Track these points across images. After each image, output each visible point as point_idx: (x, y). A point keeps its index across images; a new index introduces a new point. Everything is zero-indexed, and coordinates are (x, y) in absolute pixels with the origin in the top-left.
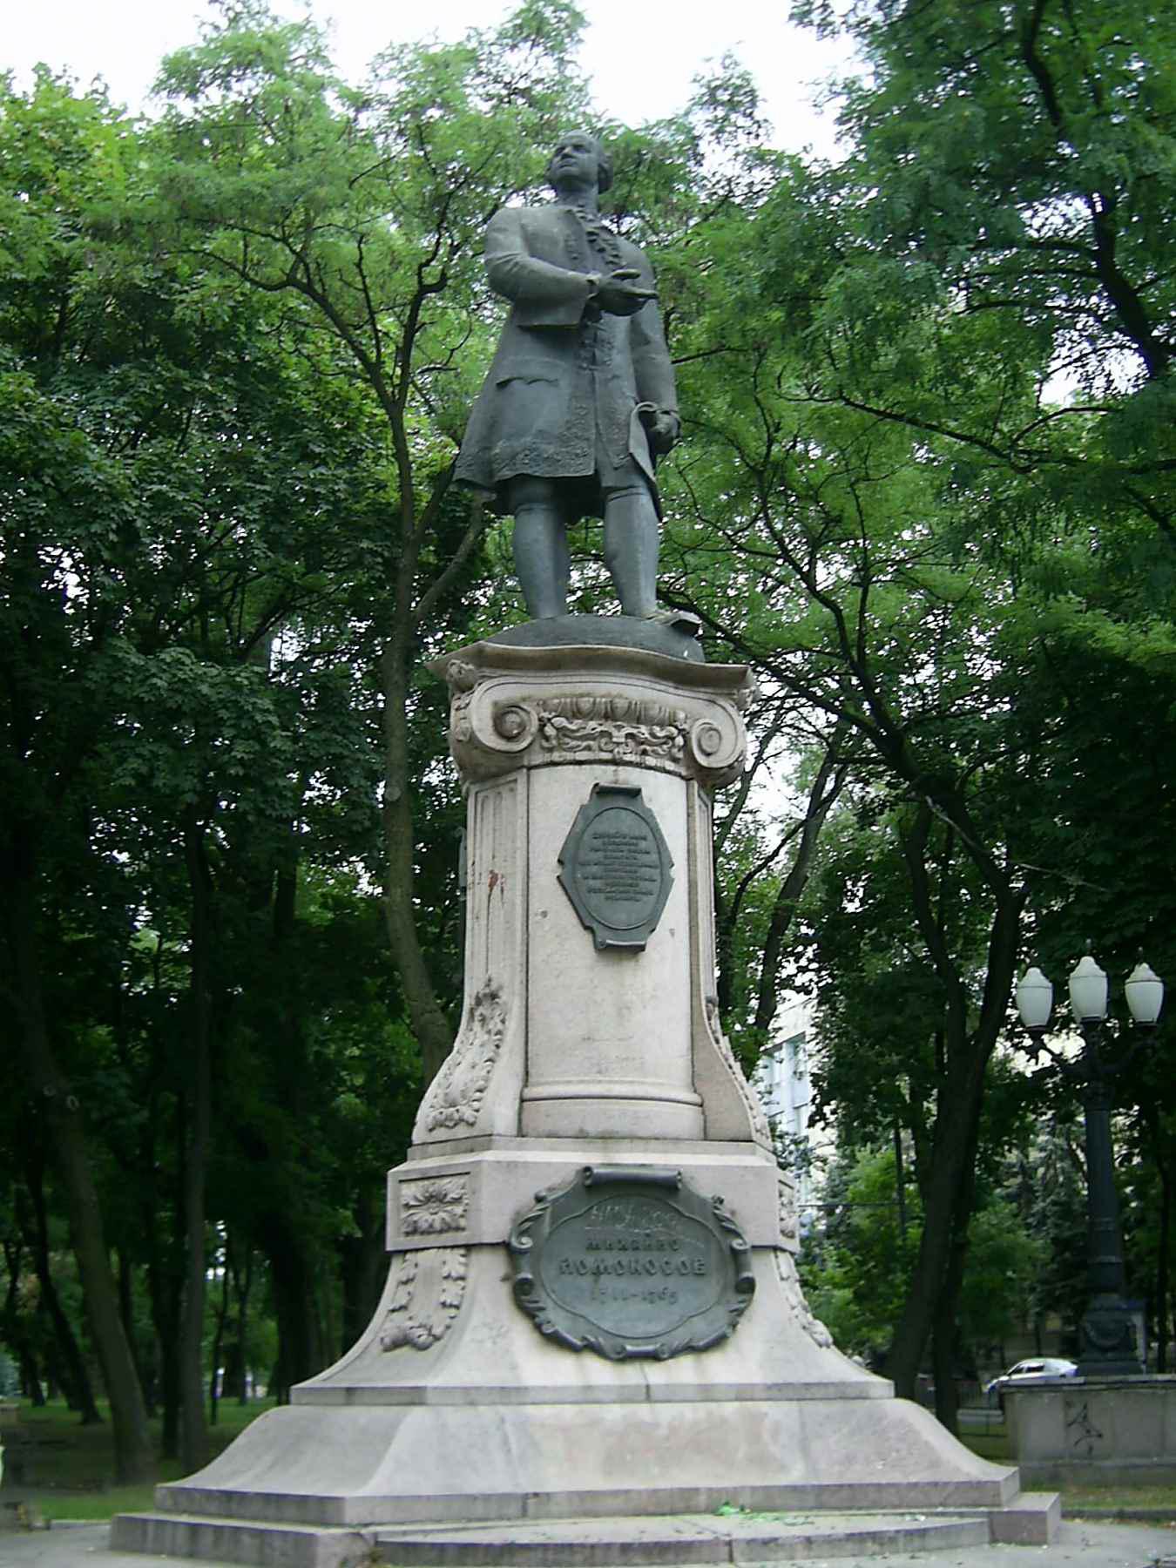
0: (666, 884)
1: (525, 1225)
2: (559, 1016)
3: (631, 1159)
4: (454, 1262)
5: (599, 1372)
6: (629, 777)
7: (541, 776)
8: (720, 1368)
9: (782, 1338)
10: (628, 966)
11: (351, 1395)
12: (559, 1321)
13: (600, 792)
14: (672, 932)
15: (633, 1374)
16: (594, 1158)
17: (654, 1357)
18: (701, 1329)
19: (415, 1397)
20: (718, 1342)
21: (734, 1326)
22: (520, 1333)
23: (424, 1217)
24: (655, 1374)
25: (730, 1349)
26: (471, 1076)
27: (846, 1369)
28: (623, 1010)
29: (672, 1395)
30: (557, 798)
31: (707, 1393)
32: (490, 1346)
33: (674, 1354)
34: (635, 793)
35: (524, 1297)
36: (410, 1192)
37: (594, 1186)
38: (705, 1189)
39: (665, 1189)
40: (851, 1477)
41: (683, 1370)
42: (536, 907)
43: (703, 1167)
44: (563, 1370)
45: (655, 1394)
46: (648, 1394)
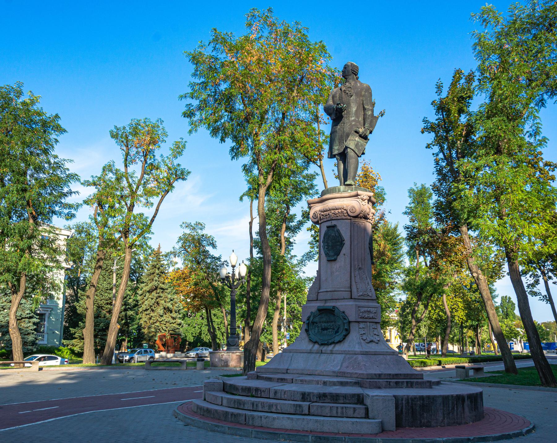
5: (317, 346)
8: (338, 347)
10: (333, 263)
13: (328, 227)
14: (344, 255)
18: (337, 339)
20: (340, 342)
21: (344, 339)
24: (324, 348)
25: (342, 344)
33: (331, 344)
34: (334, 226)
41: (330, 347)
45: (323, 352)
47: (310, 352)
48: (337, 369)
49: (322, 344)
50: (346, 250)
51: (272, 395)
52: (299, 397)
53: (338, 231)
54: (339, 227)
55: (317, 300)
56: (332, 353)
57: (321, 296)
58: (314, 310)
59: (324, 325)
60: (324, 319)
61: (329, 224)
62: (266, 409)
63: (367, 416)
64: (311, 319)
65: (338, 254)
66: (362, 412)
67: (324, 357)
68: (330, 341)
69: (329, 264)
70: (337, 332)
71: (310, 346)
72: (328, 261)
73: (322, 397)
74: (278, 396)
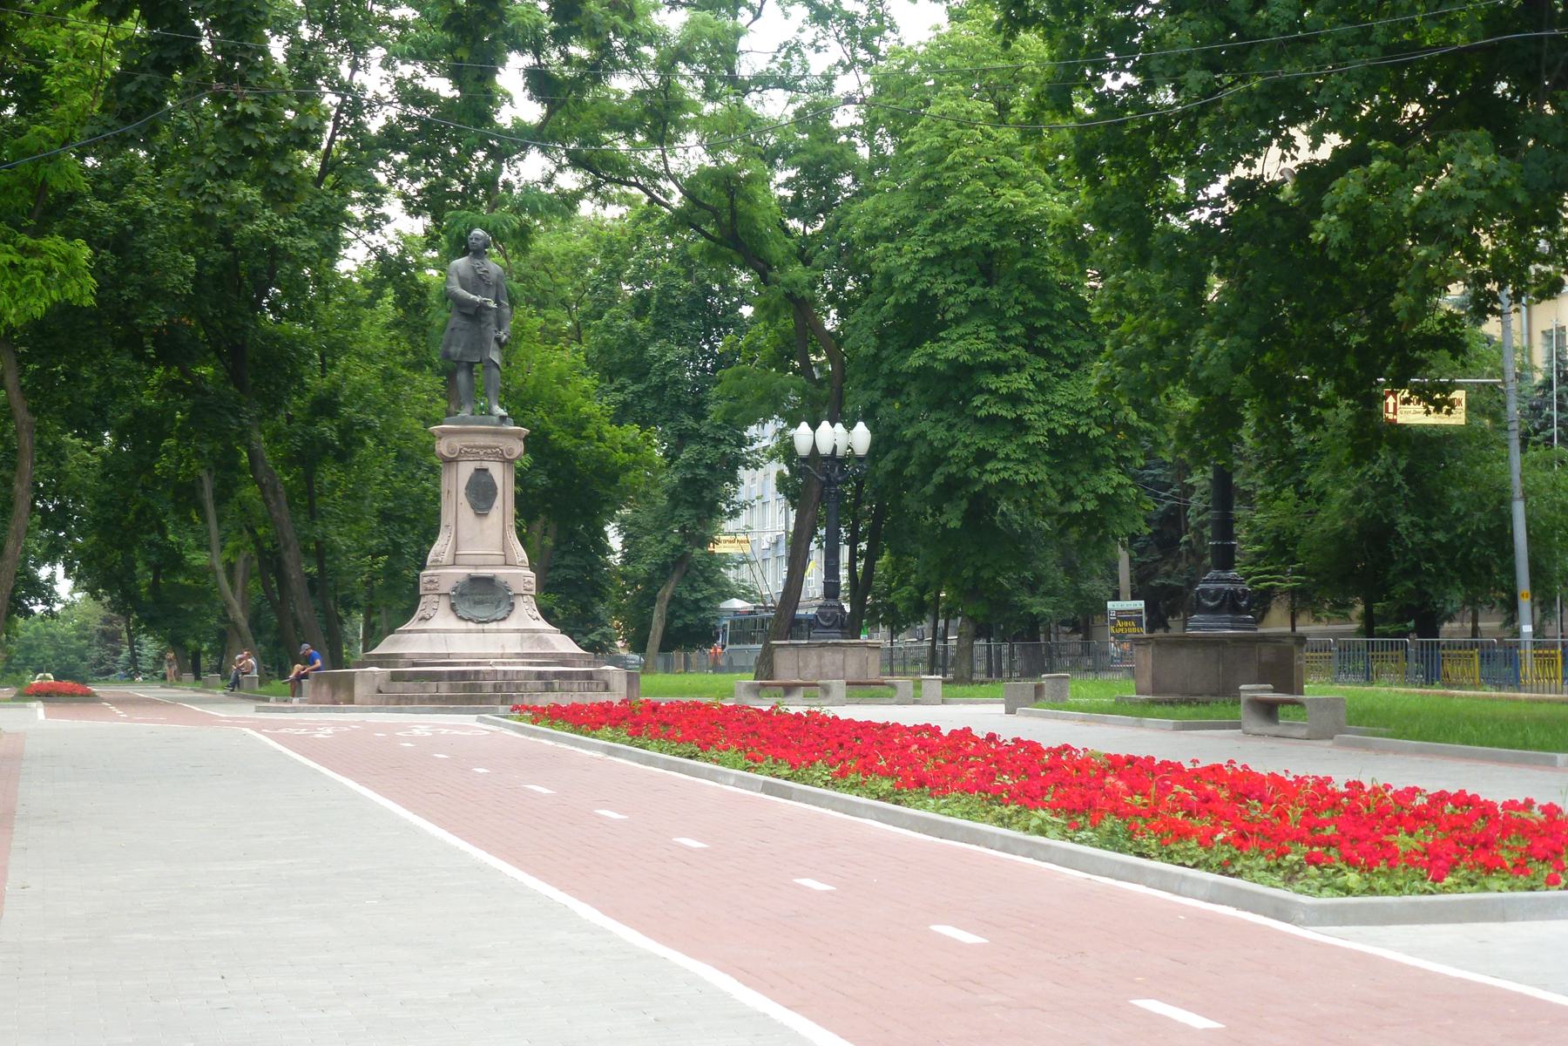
0: (495, 494)
2: (464, 533)
4: (436, 598)
5: (471, 625)
6: (485, 465)
8: (502, 625)
9: (527, 615)
11: (409, 631)
13: (477, 470)
15: (480, 626)
16: (472, 571)
18: (500, 615)
22: (452, 617)
24: (486, 626)
26: (440, 548)
27: (543, 624)
29: (490, 631)
30: (466, 470)
31: (498, 631)
34: (486, 470)
35: (453, 608)
37: (475, 581)
38: (503, 579)
39: (489, 581)
41: (493, 626)
43: (501, 572)
44: (463, 625)
46: (484, 631)
47: (469, 631)
48: (518, 651)
50: (498, 502)
56: (498, 631)
57: (460, 560)
58: (461, 579)
61: (477, 465)
63: (607, 688)
65: (490, 507)
66: (602, 686)
73: (557, 675)
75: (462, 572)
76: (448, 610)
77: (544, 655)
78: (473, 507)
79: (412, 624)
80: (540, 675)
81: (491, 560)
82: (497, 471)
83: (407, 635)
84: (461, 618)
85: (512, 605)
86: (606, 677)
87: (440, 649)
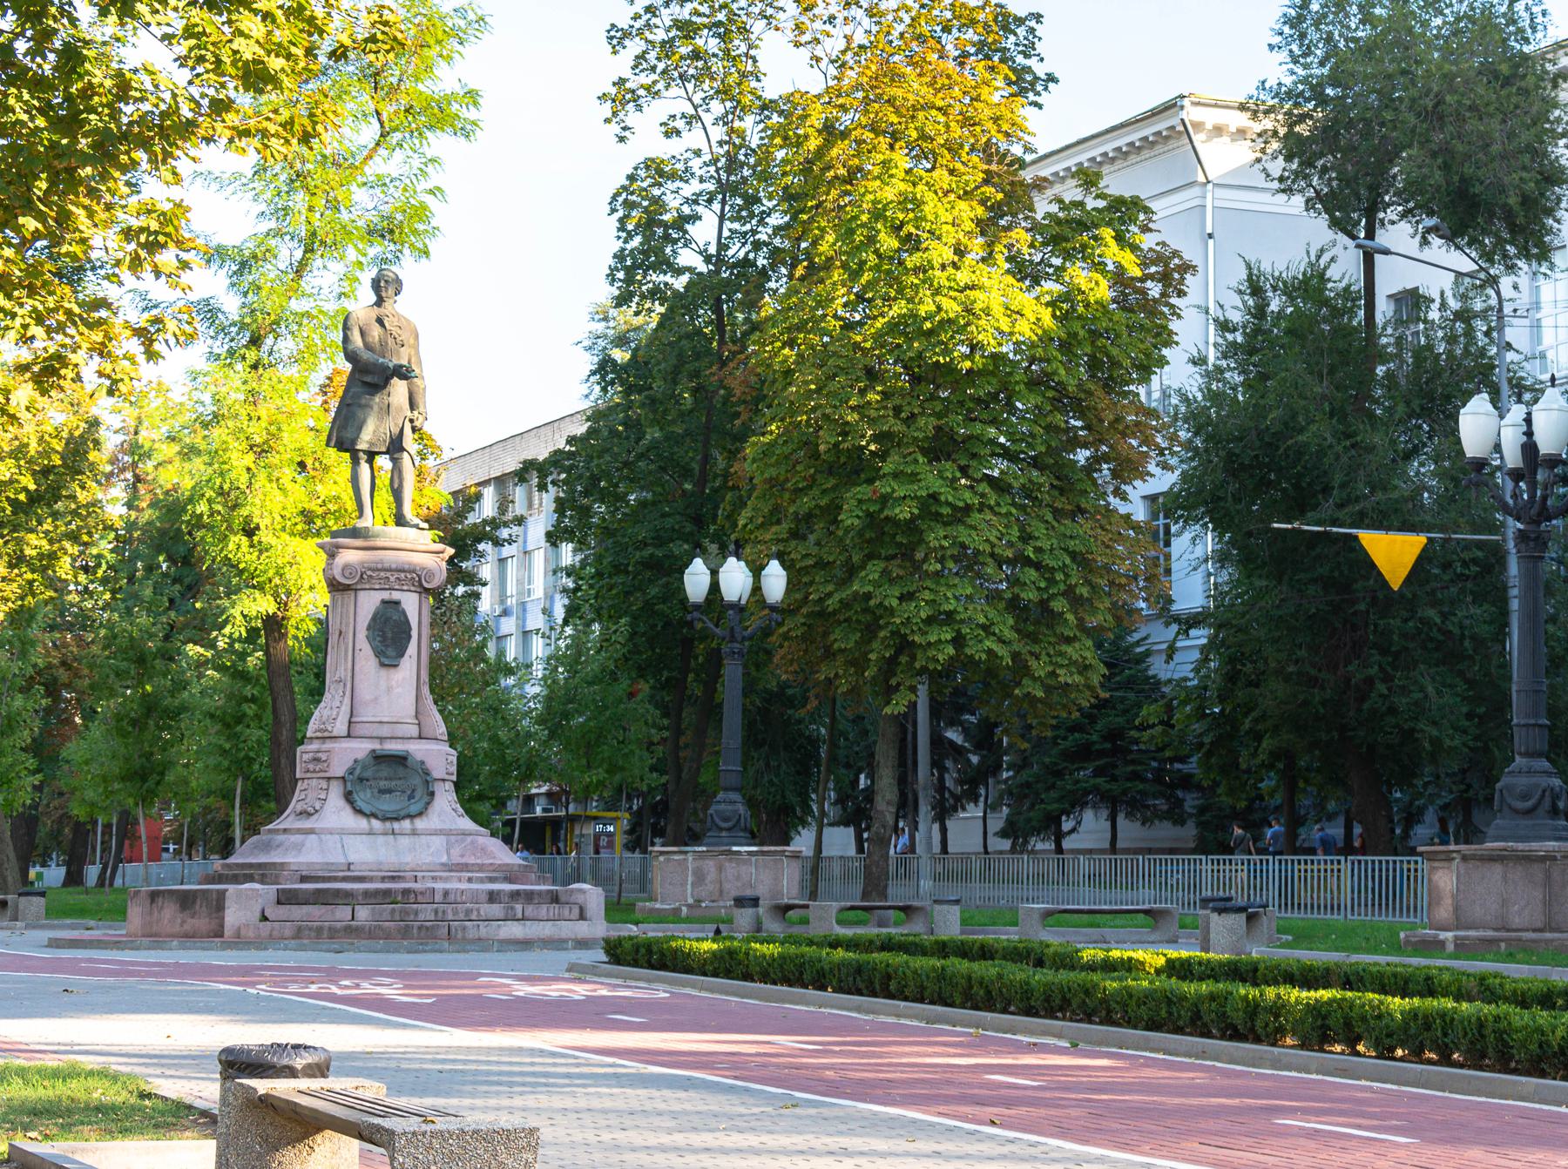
1: (351, 771)
2: (365, 691)
3: (393, 747)
5: (376, 824)
6: (396, 595)
7: (361, 594)
8: (420, 824)
9: (446, 809)
10: (392, 670)
12: (360, 804)
13: (384, 602)
15: (388, 824)
16: (376, 746)
17: (397, 819)
18: (414, 809)
19: (311, 831)
20: (420, 814)
23: (311, 767)
24: (396, 825)
26: (329, 713)
27: (467, 824)
28: (389, 689)
32: (336, 813)
34: (397, 603)
35: (348, 797)
36: (306, 757)
39: (401, 760)
40: (463, 861)
41: (406, 824)
42: (358, 647)
43: (417, 749)
47: (371, 833)
48: (444, 859)
49: (385, 819)
50: (412, 649)
51: (438, 898)
52: (484, 897)
53: (404, 613)
54: (404, 605)
55: (349, 736)
56: (414, 833)
58: (360, 756)
59: (382, 784)
60: (384, 774)
61: (386, 595)
62: (462, 916)
63: (582, 917)
64: (358, 772)
65: (402, 655)
66: (576, 911)
67: (405, 841)
68: (402, 813)
69: (384, 672)
70: (411, 797)
71: (363, 823)
72: (382, 665)
74: (451, 898)
75: (360, 749)
76: (342, 803)
77: (481, 868)
78: (379, 654)
79: (287, 821)
80: (493, 897)
81: (402, 730)
82: (411, 603)
83: (281, 838)
84: (359, 812)
85: (432, 794)
86: (580, 899)
87: (337, 858)
